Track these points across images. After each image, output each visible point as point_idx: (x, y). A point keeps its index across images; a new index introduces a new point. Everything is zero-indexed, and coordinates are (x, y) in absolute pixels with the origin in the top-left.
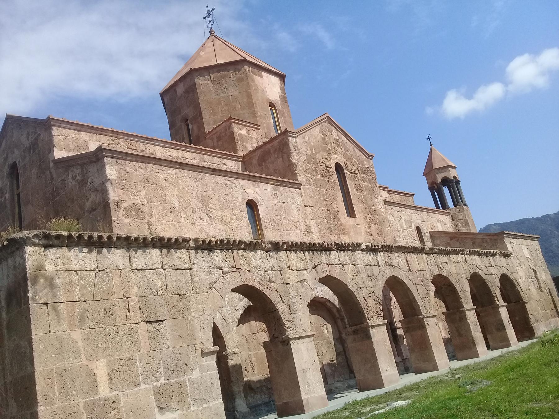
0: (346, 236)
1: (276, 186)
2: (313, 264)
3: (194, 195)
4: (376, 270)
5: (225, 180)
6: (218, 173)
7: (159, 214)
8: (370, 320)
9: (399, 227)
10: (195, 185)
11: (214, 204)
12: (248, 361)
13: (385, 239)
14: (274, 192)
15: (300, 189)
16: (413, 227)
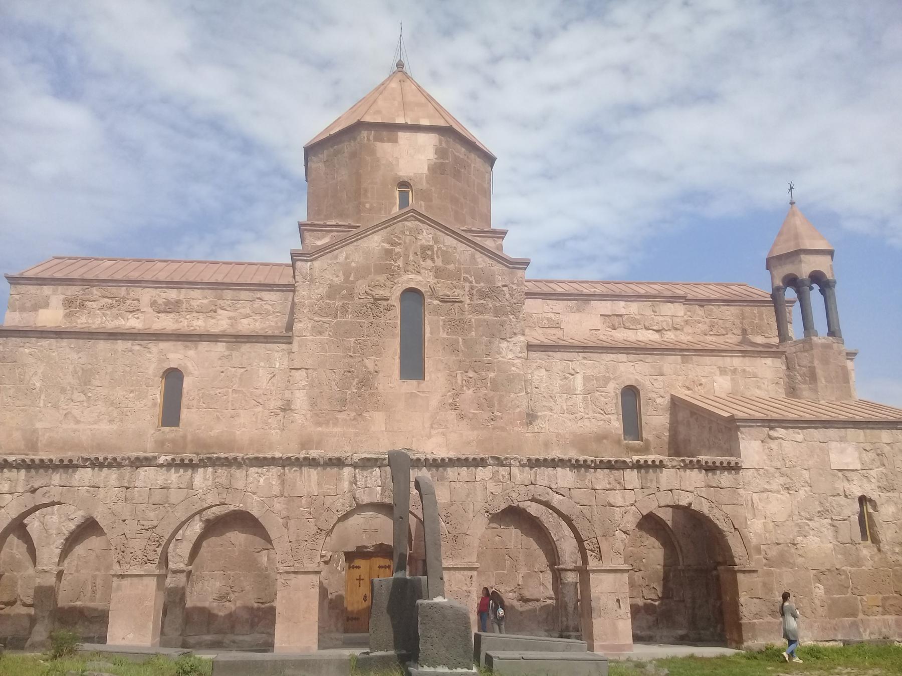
0: (381, 413)
1: (234, 344)
2: (29, 486)
3: (71, 368)
4: (175, 496)
5: (132, 345)
6: (120, 337)
7: (9, 398)
8: (122, 567)
9: (557, 389)
10: (74, 356)
11: (100, 380)
12: (90, 583)
13: (499, 414)
14: (227, 353)
15: (291, 343)
16: (613, 389)
